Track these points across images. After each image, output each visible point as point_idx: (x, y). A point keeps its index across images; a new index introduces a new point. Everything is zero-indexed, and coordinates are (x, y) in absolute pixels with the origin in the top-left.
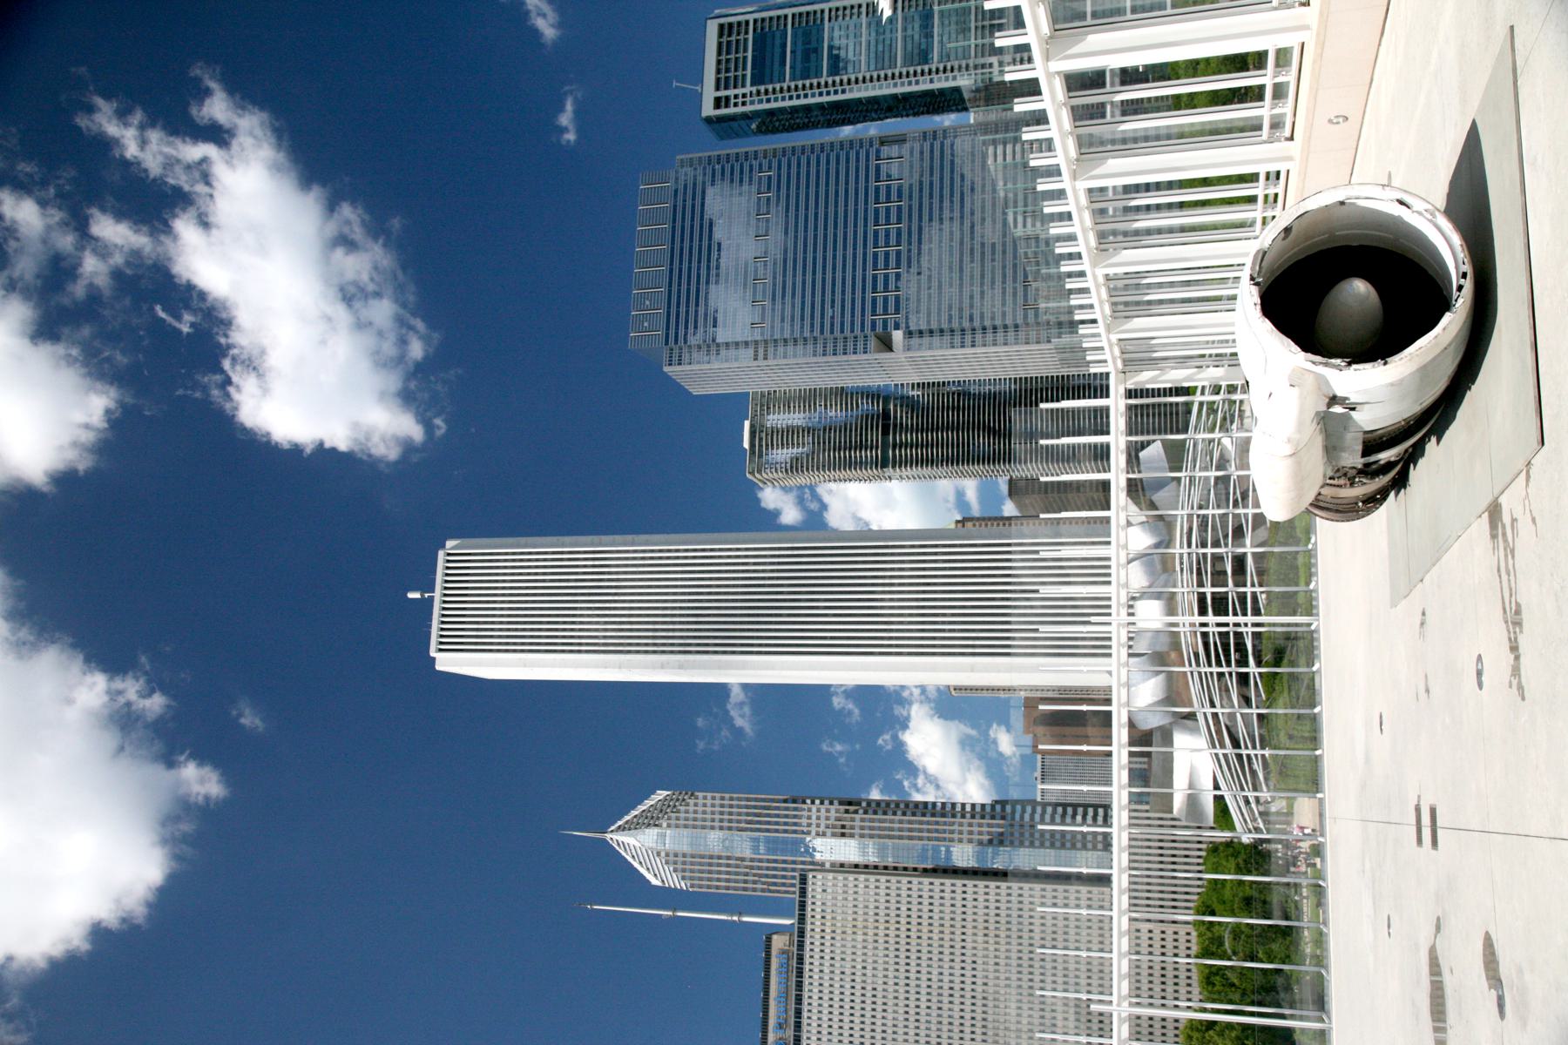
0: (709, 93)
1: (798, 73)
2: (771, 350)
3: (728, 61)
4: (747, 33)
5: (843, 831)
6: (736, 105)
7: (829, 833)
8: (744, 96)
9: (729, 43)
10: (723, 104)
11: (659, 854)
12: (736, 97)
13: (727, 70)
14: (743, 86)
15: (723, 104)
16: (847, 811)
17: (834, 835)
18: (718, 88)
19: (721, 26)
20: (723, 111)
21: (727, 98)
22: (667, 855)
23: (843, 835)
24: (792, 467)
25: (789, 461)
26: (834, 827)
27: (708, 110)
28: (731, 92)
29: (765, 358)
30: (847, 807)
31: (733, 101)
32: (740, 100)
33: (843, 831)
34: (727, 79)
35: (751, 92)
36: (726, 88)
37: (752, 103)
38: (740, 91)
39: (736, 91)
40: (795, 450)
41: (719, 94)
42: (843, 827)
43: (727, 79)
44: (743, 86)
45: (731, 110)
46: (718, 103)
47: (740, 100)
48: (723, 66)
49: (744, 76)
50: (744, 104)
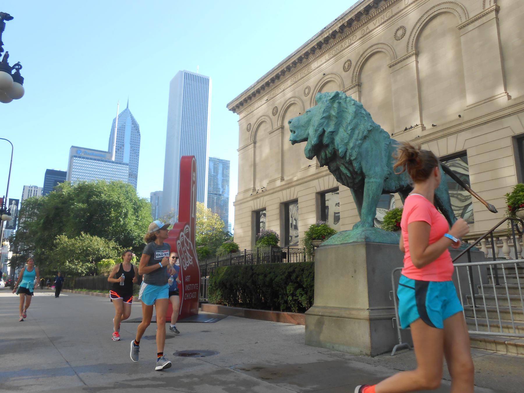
7: (130, 171)
11: (125, 123)
22: (124, 126)
26: (132, 173)
40: (213, 170)
42: (132, 175)
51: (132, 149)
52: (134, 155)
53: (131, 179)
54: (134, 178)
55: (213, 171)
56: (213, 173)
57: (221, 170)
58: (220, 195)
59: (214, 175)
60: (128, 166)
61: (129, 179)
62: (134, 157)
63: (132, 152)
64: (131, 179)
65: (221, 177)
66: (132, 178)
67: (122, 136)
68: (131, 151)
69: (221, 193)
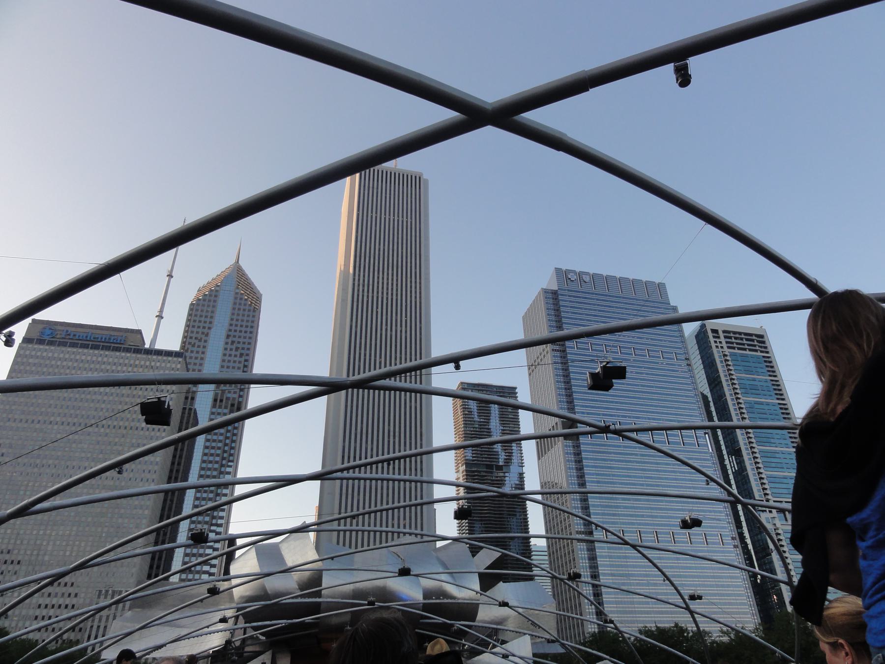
1: (742, 381)
2: (558, 354)
3: (742, 339)
4: (762, 352)
5: (218, 401)
8: (722, 347)
9: (753, 340)
10: (714, 335)
13: (736, 338)
15: (714, 335)
16: (233, 405)
17: (216, 395)
18: (724, 332)
20: (710, 334)
21: (719, 337)
22: (217, 291)
23: (215, 400)
24: (465, 408)
25: (469, 407)
28: (722, 339)
29: (553, 350)
30: (236, 406)
31: (718, 340)
32: (719, 345)
33: (218, 401)
34: (730, 338)
36: (725, 337)
37: (719, 352)
38: (724, 345)
42: (221, 401)
43: (730, 338)
44: (729, 347)
45: (712, 340)
46: (715, 331)
47: (719, 345)
48: (737, 336)
49: (734, 348)
50: (717, 347)
51: (230, 341)
52: (233, 353)
53: (220, 410)
54: (226, 407)
55: (476, 413)
56: (477, 419)
57: (497, 412)
58: (500, 468)
59: (481, 422)
60: (180, 359)
61: (214, 410)
62: (232, 359)
63: (229, 346)
64: (220, 410)
65: (498, 425)
66: (220, 407)
67: (209, 314)
68: (227, 343)
69: (501, 464)
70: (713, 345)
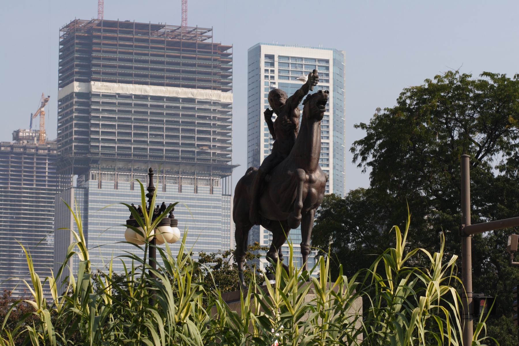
0: (277, 51)
6: (266, 71)
8: (273, 77)
12: (273, 71)
14: (280, 77)
18: (280, 57)
19: (327, 61)
20: (263, 60)
21: (272, 64)
27: (265, 50)
31: (270, 69)
32: (270, 74)
35: (274, 83)
38: (276, 75)
39: (276, 72)
41: (276, 59)
44: (280, 77)
46: (271, 57)
70: (263, 74)
